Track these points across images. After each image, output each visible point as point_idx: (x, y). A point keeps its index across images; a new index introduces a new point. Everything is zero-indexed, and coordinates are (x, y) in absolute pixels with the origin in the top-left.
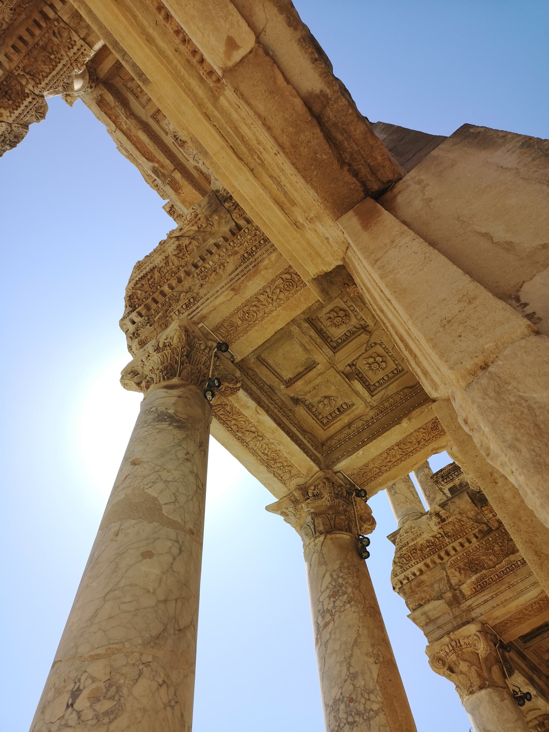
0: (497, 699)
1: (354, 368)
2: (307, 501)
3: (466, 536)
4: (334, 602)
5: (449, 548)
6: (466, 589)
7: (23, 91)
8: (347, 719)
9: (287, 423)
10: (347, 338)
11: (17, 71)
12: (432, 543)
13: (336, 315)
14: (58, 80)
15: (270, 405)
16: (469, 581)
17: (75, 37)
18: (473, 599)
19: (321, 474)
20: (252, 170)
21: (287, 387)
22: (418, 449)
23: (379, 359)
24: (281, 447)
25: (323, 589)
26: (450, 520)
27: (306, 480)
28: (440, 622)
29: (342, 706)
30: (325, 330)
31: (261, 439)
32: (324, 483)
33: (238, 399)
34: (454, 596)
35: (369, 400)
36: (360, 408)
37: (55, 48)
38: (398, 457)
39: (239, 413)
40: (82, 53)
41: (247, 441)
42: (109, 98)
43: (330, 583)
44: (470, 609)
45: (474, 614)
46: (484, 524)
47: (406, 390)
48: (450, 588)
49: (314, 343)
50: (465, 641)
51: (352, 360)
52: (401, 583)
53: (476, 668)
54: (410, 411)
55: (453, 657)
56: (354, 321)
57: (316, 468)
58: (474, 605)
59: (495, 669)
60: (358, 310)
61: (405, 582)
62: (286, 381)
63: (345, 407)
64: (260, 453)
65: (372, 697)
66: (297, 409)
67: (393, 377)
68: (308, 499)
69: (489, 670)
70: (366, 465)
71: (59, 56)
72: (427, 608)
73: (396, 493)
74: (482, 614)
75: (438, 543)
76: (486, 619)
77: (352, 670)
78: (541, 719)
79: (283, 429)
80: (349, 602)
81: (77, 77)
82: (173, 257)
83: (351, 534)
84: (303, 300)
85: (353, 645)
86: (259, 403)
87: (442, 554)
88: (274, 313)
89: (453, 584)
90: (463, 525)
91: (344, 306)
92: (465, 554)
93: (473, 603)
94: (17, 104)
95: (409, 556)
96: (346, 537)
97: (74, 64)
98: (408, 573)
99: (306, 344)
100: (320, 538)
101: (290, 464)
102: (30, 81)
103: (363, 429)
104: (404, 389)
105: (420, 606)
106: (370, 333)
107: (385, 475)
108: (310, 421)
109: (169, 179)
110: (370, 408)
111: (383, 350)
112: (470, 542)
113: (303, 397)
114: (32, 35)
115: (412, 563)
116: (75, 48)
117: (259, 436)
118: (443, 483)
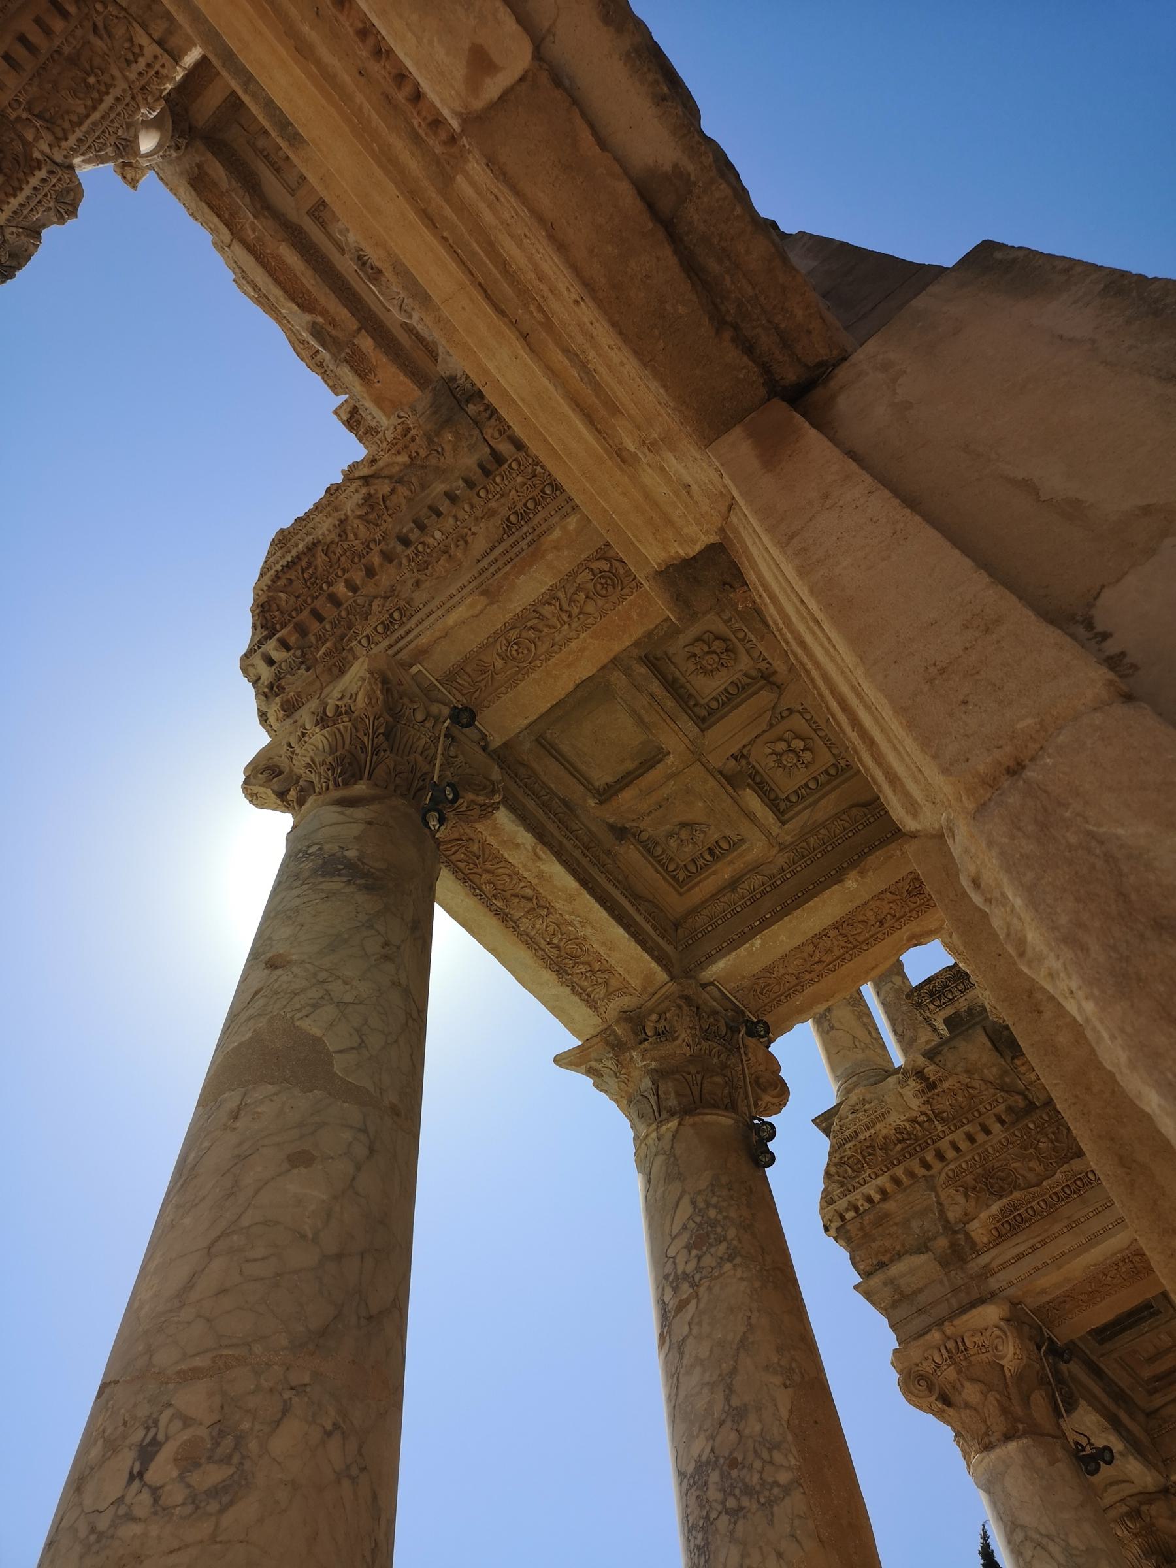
0: (1041, 1461)
1: (744, 762)
2: (642, 1046)
3: (980, 1120)
4: (699, 1258)
5: (944, 1144)
6: (980, 1231)
7: (28, 156)
8: (723, 1503)
9: (601, 879)
10: (730, 699)
11: (14, 109)
12: (908, 1133)
13: (706, 649)
14: (103, 132)
15: (565, 841)
16: (984, 1215)
17: (142, 39)
18: (994, 1252)
19: (672, 987)
20: (525, 337)
21: (601, 803)
22: (880, 935)
23: (798, 744)
24: (588, 931)
25: (674, 1233)
26: (946, 1085)
27: (642, 1001)
28: (922, 1299)
29: (714, 1477)
30: (683, 680)
31: (545, 912)
32: (679, 1007)
33: (495, 828)
34: (953, 1245)
35: (775, 830)
36: (756, 848)
37: (97, 61)
38: (837, 953)
39: (499, 859)
40: (157, 72)
41: (515, 918)
42: (218, 171)
43: (690, 1218)
44: (987, 1272)
45: (993, 1284)
46: (1019, 1093)
47: (854, 811)
48: (945, 1228)
49: (659, 709)
50: (976, 1339)
51: (740, 746)
52: (842, 1218)
53: (998, 1396)
54: (863, 856)
55: (951, 1373)
56: (745, 663)
57: (662, 976)
58: (994, 1265)
59: (1039, 1399)
60: (754, 640)
61: (850, 1215)
62: (598, 790)
63: (725, 846)
64: (543, 944)
65: (778, 1457)
66: (622, 850)
67: (828, 782)
68: (645, 1040)
69: (1026, 1401)
70: (769, 969)
71: (106, 78)
72: (895, 1270)
73: (832, 1028)
74: (1011, 1284)
76: (1020, 1293)
77: (735, 1402)
78: (1133, 1503)
79: (592, 892)
80: (730, 1259)
81: (148, 125)
82: (357, 521)
83: (734, 1115)
84: (635, 617)
85: (738, 1349)
86: (541, 836)
87: (930, 1157)
88: (573, 645)
89: (952, 1220)
90: (973, 1097)
91: (722, 629)
92: (977, 1158)
93: (994, 1259)
94: (16, 184)
95: (859, 1161)
96: (724, 1120)
97: (139, 98)
98: (857, 1196)
99: (642, 712)
100: (670, 1124)
101: (607, 966)
102: (43, 132)
103: (764, 893)
104: (850, 807)
105: (882, 1265)
106: (779, 687)
107: (809, 991)
108: (649, 876)
109: (347, 350)
110: (777, 848)
112: (987, 1132)
113: (635, 824)
114: (48, 32)
116: (142, 63)
117: (540, 906)
118: (932, 1007)
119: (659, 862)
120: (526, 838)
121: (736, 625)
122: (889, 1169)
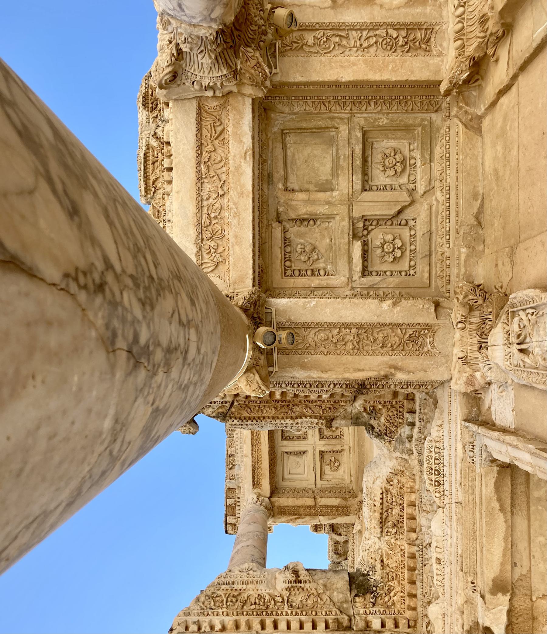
12: (264, 602)
13: (393, 154)
24: (234, 221)
26: (307, 585)
35: (356, 276)
46: (348, 616)
49: (351, 162)
52: (187, 628)
56: (404, 180)
63: (322, 273)
75: (271, 607)
84: (390, 68)
87: (269, 622)
95: (222, 601)
99: (342, 157)
111: (408, 238)
115: (220, 611)
119: (285, 255)
120: (248, 141)
121: (414, 154)
122: (237, 615)
